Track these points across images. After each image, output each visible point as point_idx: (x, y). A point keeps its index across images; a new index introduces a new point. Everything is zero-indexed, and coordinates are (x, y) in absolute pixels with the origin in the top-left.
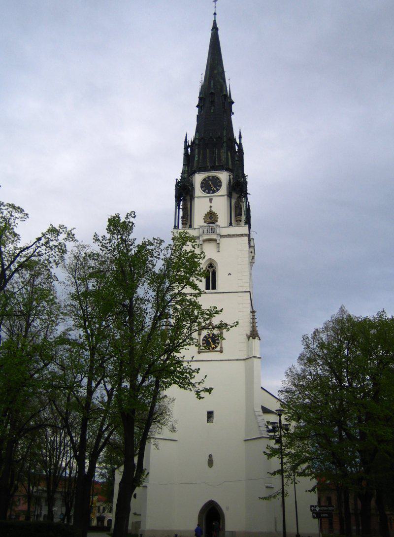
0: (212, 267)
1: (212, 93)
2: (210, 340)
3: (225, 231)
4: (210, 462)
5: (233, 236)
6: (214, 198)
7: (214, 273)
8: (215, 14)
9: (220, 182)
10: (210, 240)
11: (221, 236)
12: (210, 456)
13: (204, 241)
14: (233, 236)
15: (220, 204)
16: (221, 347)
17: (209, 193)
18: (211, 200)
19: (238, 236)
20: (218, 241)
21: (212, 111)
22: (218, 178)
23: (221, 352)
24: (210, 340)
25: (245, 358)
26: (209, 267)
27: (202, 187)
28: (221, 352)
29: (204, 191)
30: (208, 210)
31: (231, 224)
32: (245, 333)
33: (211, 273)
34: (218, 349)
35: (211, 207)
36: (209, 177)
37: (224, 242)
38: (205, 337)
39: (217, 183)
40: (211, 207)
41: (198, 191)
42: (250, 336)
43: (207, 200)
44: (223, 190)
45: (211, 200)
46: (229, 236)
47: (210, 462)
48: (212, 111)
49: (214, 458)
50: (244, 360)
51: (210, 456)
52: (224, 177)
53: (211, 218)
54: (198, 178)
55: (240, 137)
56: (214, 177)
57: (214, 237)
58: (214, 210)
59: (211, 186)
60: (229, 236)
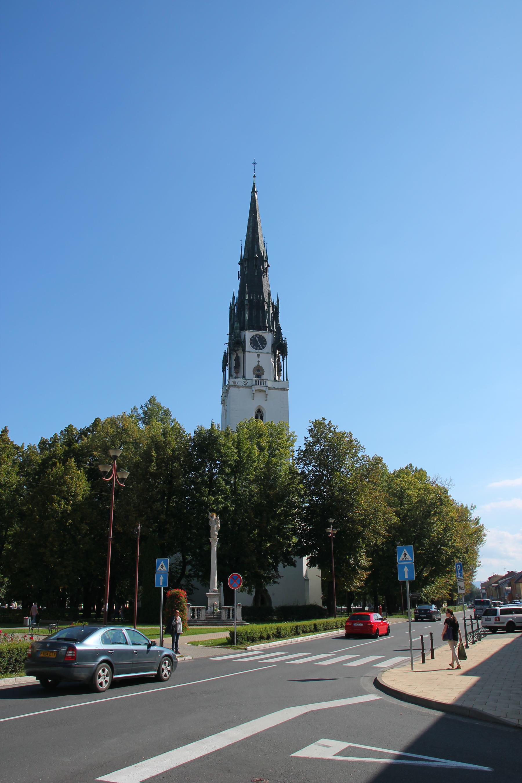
3: (269, 384)
5: (277, 389)
8: (254, 177)
9: (265, 341)
10: (260, 391)
11: (269, 388)
13: (256, 391)
14: (277, 389)
15: (266, 359)
17: (256, 349)
18: (258, 356)
19: (281, 389)
20: (266, 393)
26: (258, 412)
27: (251, 343)
29: (253, 347)
30: (257, 364)
35: (259, 362)
36: (256, 335)
39: (263, 341)
40: (259, 362)
45: (258, 356)
46: (274, 389)
48: (256, 274)
52: (269, 337)
53: (259, 372)
55: (278, 301)
56: (260, 336)
57: (263, 388)
58: (261, 364)
59: (258, 343)
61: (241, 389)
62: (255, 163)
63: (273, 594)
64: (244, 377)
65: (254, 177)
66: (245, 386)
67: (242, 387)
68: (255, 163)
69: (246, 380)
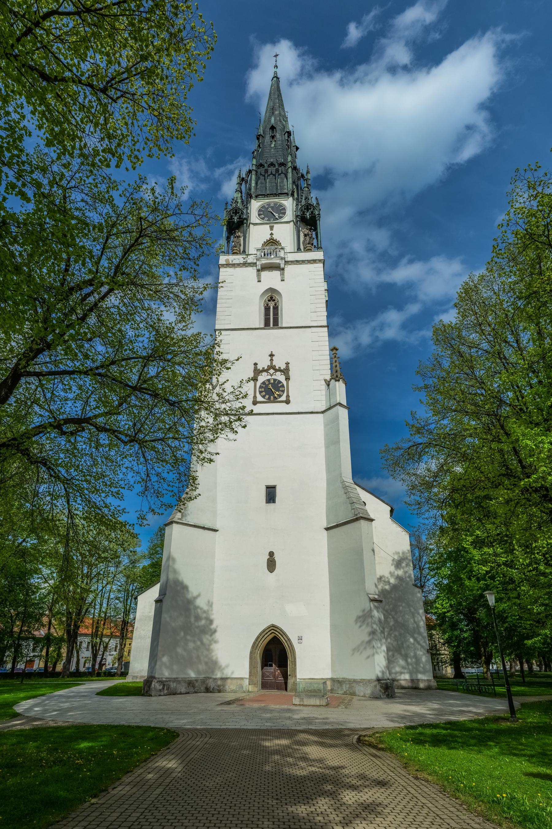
0: (274, 300)
1: (273, 128)
2: (270, 386)
3: (290, 257)
4: (271, 565)
5: (303, 262)
6: (275, 226)
7: (276, 308)
11: (287, 263)
12: (271, 554)
14: (303, 262)
16: (288, 396)
18: (272, 228)
21: (273, 146)
22: (281, 205)
23: (288, 402)
24: (270, 386)
25: (323, 410)
28: (288, 402)
29: (263, 219)
30: (268, 237)
31: (299, 249)
32: (322, 378)
33: (272, 307)
34: (284, 398)
36: (269, 204)
37: (289, 269)
38: (264, 383)
40: (272, 234)
41: (254, 217)
42: (331, 380)
43: (267, 227)
44: (289, 215)
45: (272, 228)
46: (297, 262)
47: (271, 565)
48: (273, 146)
49: (277, 557)
50: (323, 412)
51: (271, 554)
54: (255, 205)
56: (275, 204)
58: (275, 237)
59: (271, 215)
60: (297, 262)
61: (238, 270)
62: (276, 56)
63: (300, 638)
64: (244, 251)
65: (276, 66)
66: (245, 264)
67: (239, 265)
68: (276, 56)
69: (247, 255)
